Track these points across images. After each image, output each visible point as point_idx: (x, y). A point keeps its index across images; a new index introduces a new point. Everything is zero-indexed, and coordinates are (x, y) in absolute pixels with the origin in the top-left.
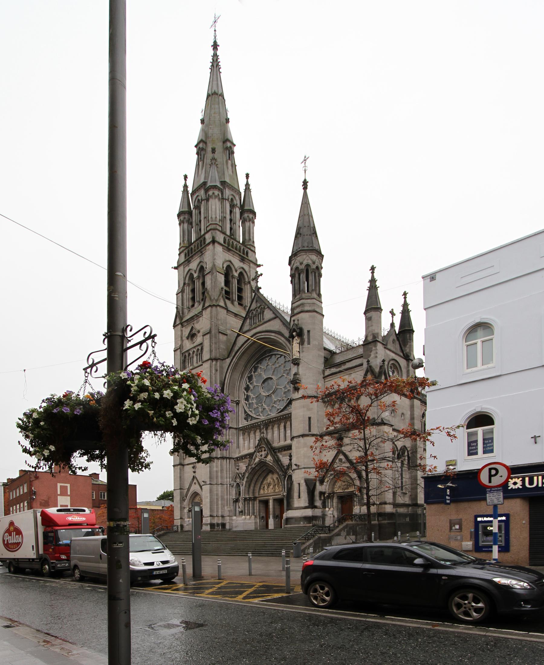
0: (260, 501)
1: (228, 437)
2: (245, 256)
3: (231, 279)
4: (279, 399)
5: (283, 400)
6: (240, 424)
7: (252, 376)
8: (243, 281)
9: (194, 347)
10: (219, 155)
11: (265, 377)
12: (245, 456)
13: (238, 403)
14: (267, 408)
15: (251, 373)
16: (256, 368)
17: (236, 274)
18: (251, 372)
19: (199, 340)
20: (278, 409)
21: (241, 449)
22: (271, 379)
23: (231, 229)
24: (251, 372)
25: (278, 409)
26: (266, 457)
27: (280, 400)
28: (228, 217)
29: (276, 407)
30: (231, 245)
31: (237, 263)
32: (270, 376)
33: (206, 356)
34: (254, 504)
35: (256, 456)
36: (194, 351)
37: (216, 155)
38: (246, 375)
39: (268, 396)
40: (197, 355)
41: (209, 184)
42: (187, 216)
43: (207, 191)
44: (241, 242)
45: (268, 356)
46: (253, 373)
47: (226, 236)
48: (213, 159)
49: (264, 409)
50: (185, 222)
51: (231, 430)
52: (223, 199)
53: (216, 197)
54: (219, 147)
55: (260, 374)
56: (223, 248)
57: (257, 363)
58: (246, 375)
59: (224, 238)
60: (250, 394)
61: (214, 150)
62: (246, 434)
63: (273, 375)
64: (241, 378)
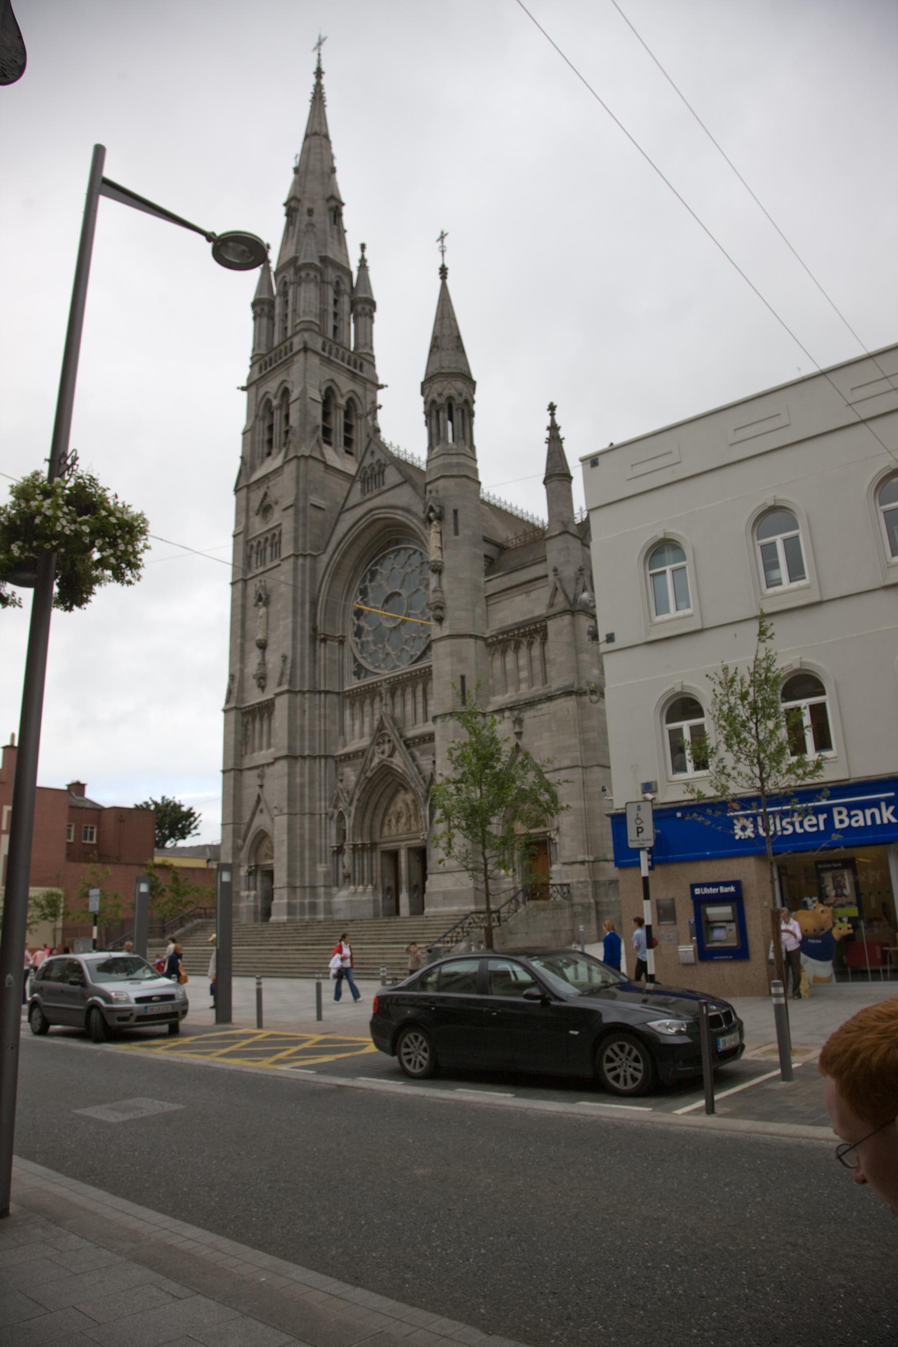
0: (384, 853)
1: (322, 710)
2: (357, 371)
4: (414, 635)
5: (420, 638)
6: (346, 683)
7: (366, 588)
8: (354, 414)
9: (268, 531)
10: (322, 219)
11: (389, 592)
12: (356, 755)
13: (342, 642)
14: (393, 653)
15: (365, 582)
16: (373, 574)
18: (364, 581)
19: (276, 517)
20: (412, 656)
21: (348, 737)
22: (399, 594)
23: (335, 328)
24: (364, 581)
25: (412, 656)
26: (391, 756)
27: (415, 638)
28: (331, 309)
29: (407, 651)
30: (333, 354)
31: (345, 385)
32: (397, 590)
33: (287, 549)
34: (372, 858)
35: (374, 755)
36: (267, 539)
37: (316, 218)
38: (357, 586)
39: (395, 628)
40: (272, 546)
41: (301, 261)
43: (298, 270)
44: (352, 349)
45: (393, 551)
46: (367, 583)
47: (326, 341)
48: (311, 225)
49: (388, 654)
51: (329, 696)
52: (323, 282)
54: (320, 207)
55: (380, 585)
56: (321, 360)
57: (376, 564)
58: (357, 586)
60: (363, 623)
61: (310, 212)
62: (357, 705)
63: (401, 587)
64: (348, 591)
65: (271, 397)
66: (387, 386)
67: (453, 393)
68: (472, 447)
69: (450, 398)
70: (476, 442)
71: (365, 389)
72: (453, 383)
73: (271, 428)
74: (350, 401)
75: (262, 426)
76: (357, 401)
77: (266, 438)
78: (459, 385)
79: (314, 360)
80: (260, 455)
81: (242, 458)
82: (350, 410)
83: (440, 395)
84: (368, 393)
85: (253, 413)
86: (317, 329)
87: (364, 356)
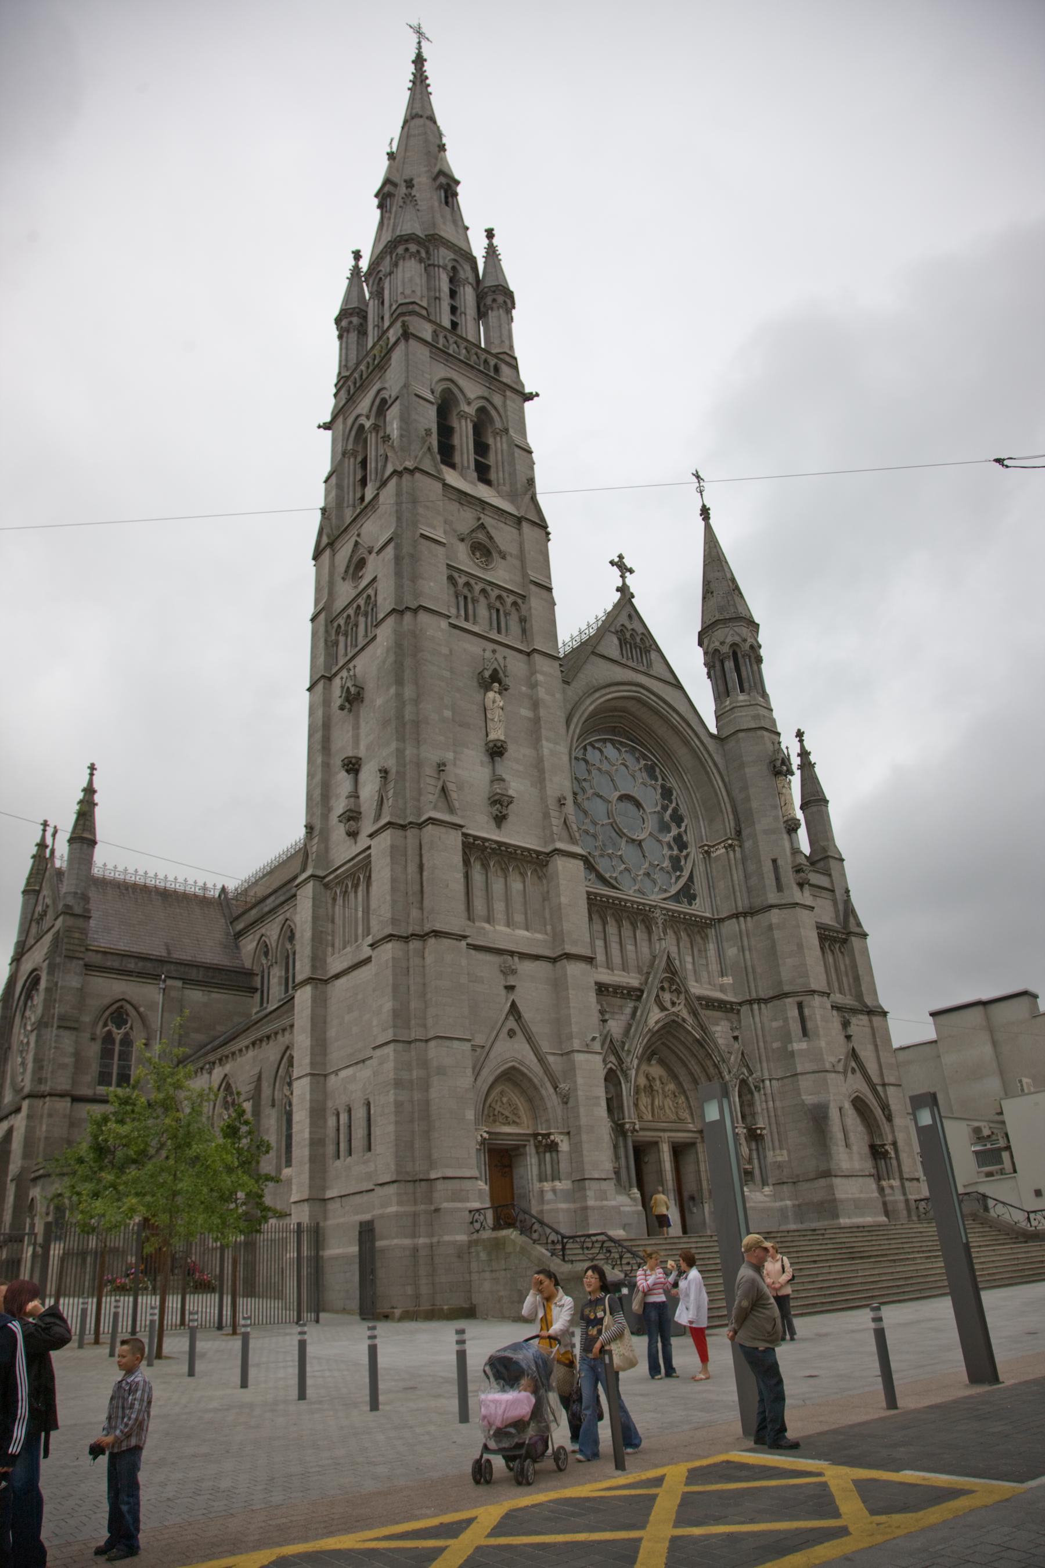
3: (455, 424)
17: (471, 410)
42: (355, 320)
50: (352, 330)
53: (412, 255)
56: (431, 352)
59: (435, 332)
65: (362, 420)
66: (537, 395)
67: (737, 639)
68: (764, 695)
69: (734, 645)
70: (769, 690)
71: (504, 396)
72: (736, 629)
73: (364, 463)
74: (482, 410)
75: (351, 465)
76: (493, 413)
77: (359, 477)
78: (745, 631)
79: (422, 353)
80: (351, 502)
81: (324, 510)
82: (482, 423)
83: (722, 643)
84: (508, 402)
85: (340, 449)
86: (424, 313)
87: (501, 356)
